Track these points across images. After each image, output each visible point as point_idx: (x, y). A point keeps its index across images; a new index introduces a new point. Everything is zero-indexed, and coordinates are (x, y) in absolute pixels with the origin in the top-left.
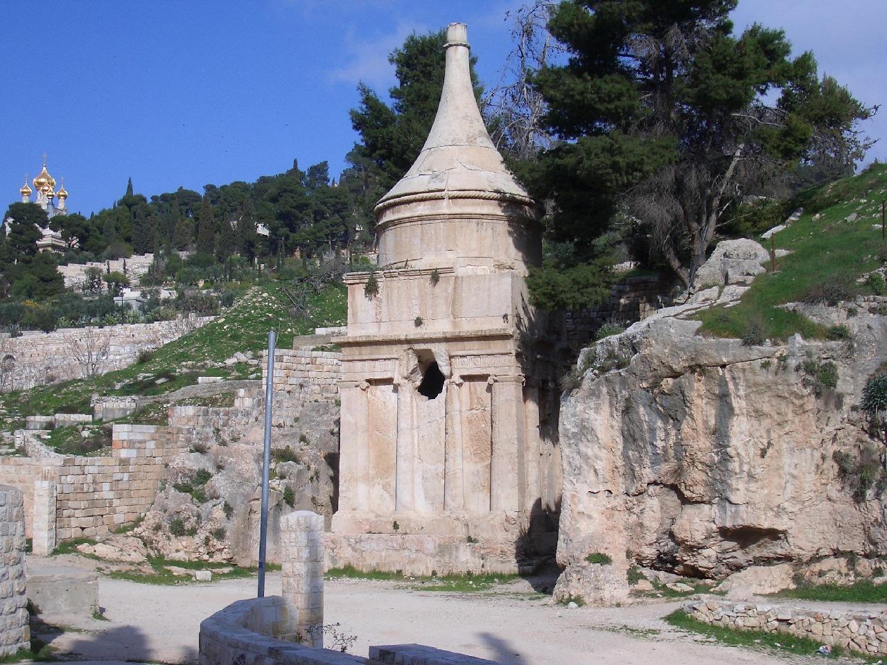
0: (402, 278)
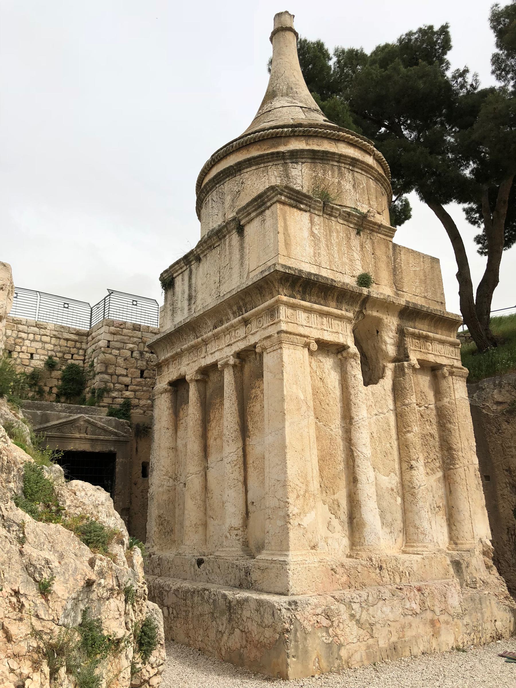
0: (341, 221)
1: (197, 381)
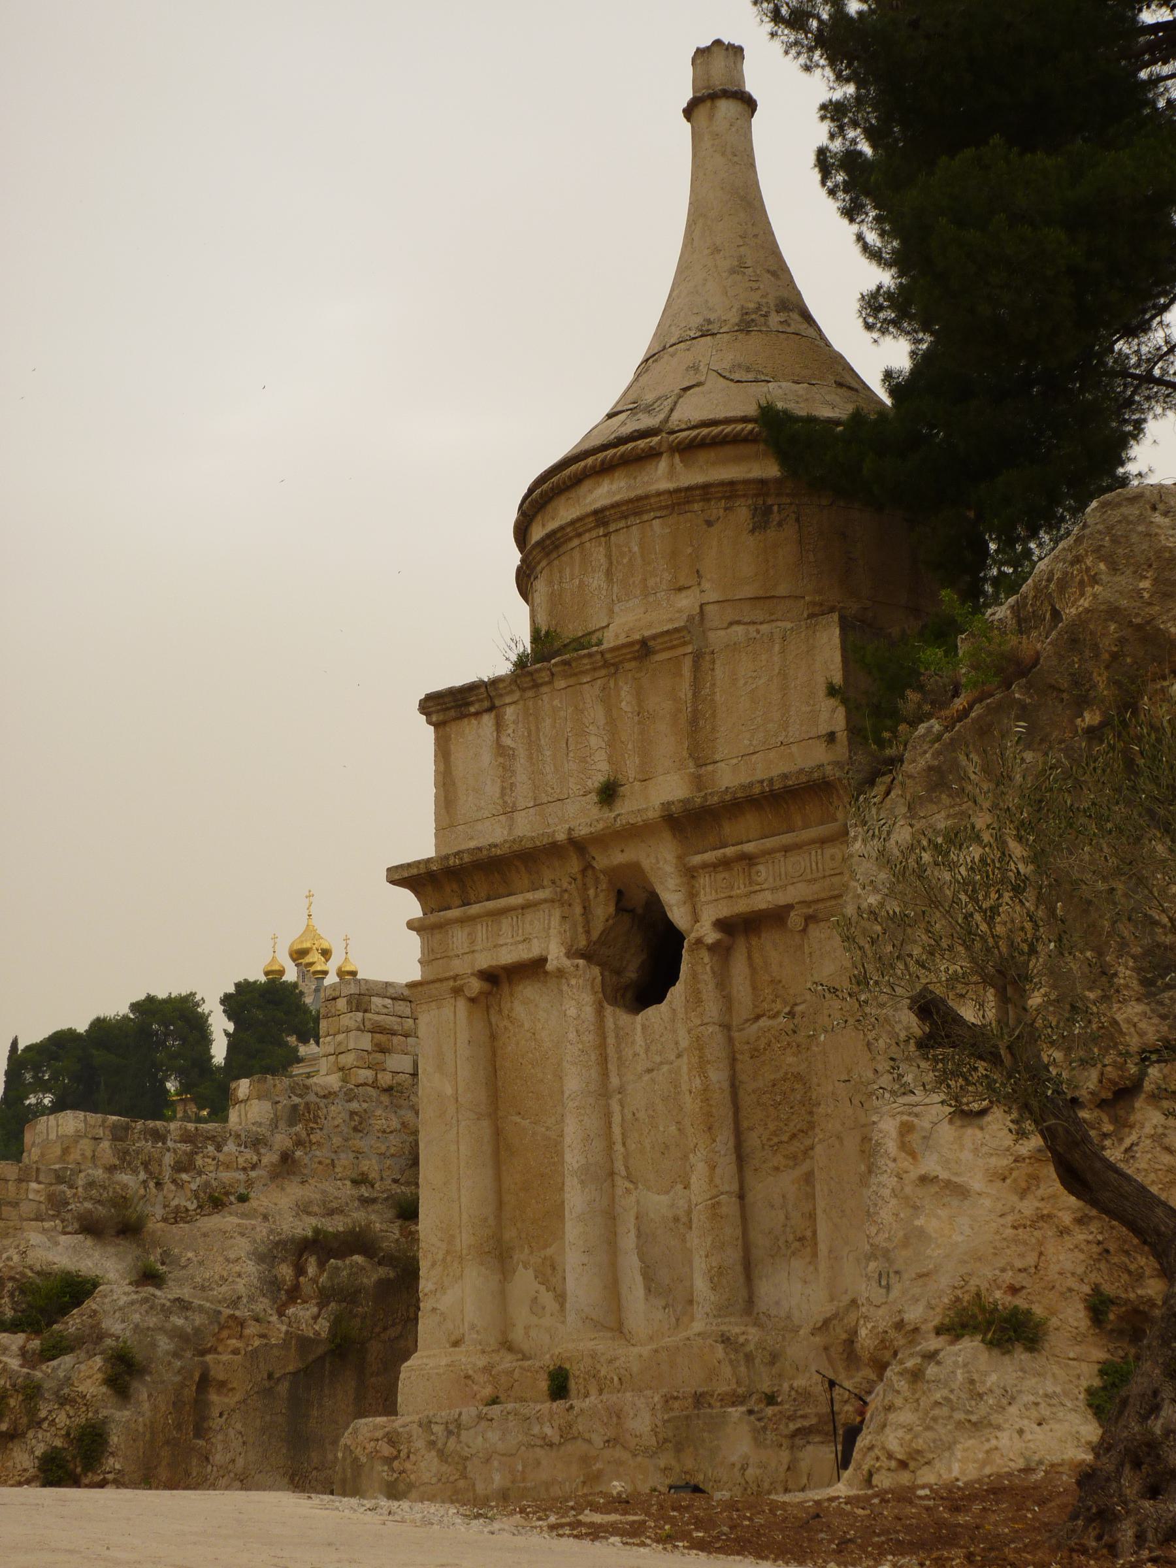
0: (561, 684)
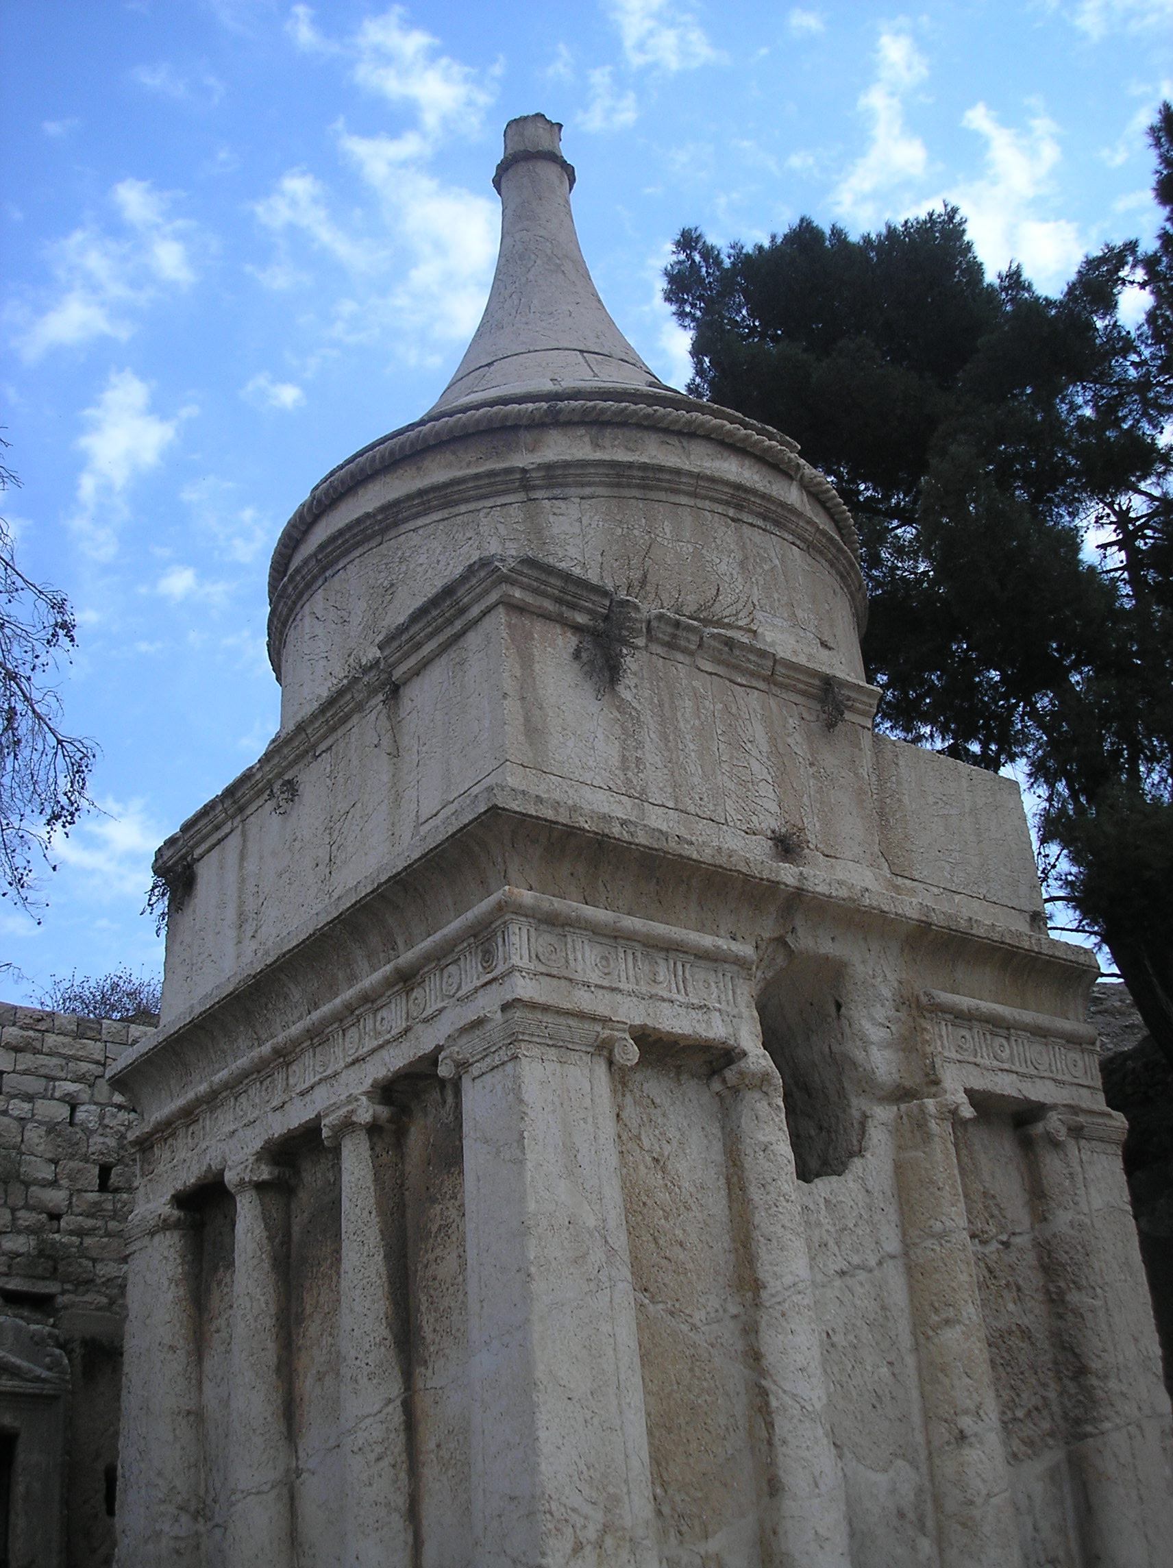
0: (709, 667)
1: (260, 1187)
